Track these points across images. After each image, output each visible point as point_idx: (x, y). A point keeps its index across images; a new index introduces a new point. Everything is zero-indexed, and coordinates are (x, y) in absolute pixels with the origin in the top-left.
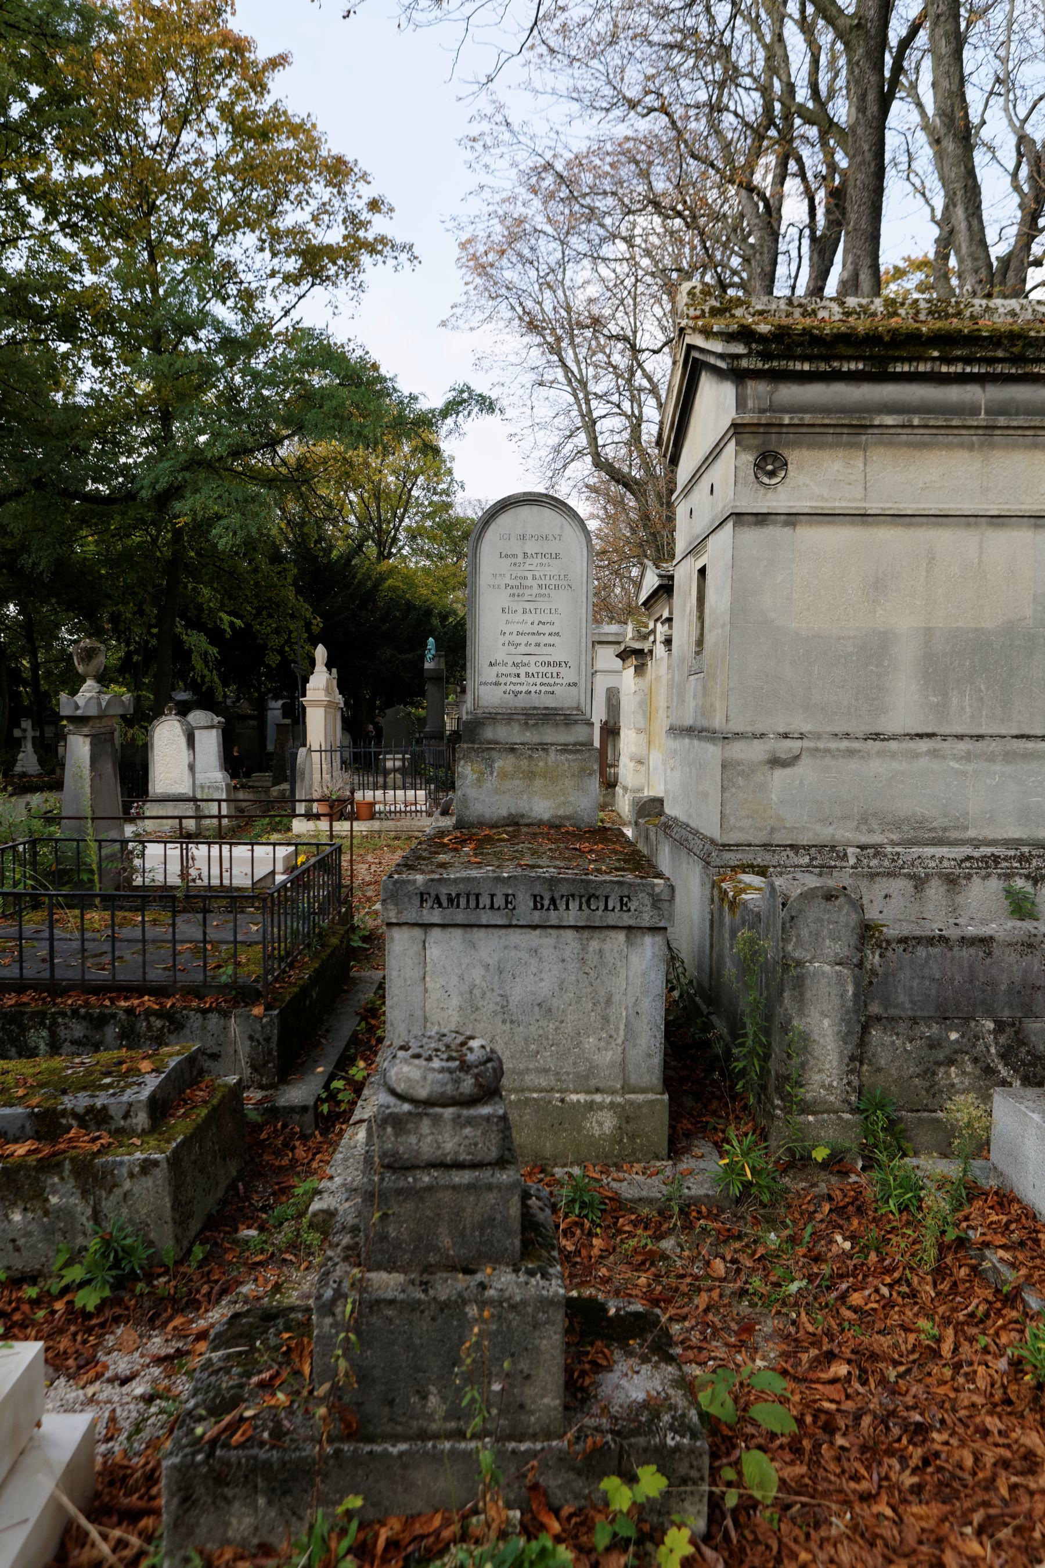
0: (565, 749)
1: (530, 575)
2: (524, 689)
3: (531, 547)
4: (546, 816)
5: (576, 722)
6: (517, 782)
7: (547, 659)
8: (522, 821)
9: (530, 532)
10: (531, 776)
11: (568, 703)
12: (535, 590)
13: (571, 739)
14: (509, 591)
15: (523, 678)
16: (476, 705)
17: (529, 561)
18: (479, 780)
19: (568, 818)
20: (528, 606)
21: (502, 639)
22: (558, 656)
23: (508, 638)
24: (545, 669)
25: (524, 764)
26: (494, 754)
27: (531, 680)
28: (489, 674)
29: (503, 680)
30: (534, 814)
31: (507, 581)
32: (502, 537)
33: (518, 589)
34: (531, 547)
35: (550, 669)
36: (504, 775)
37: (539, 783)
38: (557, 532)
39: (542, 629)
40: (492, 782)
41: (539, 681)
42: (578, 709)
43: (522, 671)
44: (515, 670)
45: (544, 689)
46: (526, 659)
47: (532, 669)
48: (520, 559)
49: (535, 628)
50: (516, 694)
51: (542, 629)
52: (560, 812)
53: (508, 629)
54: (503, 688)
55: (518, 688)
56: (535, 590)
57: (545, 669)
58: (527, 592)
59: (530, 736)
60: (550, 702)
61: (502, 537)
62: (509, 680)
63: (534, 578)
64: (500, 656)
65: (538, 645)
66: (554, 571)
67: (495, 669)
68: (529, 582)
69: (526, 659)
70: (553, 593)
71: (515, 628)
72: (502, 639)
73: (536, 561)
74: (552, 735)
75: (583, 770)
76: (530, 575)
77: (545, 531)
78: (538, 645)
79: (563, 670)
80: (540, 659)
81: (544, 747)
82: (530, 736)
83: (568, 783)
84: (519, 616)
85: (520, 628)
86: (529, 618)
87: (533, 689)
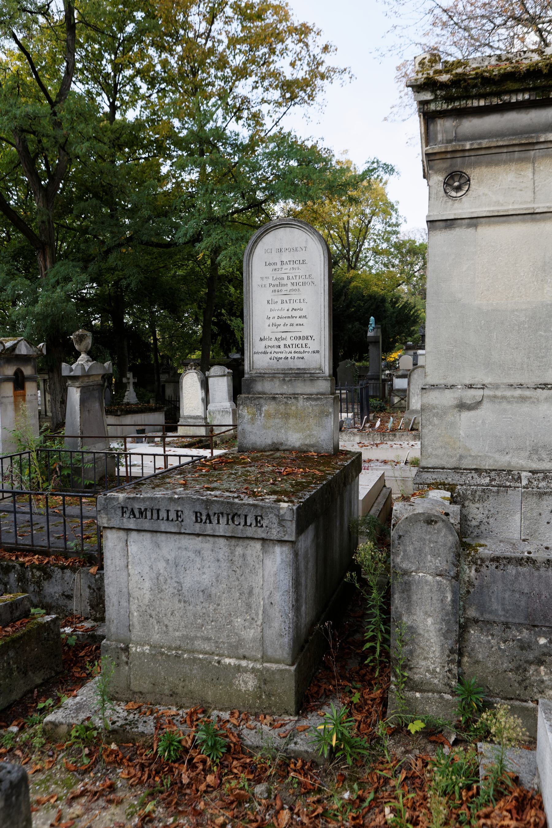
0: (310, 397)
1: (285, 276)
2: (283, 356)
3: (286, 257)
4: (297, 444)
5: (318, 378)
6: (277, 421)
7: (298, 335)
8: (282, 448)
9: (285, 246)
10: (286, 416)
11: (313, 365)
12: (290, 287)
13: (314, 390)
14: (272, 288)
15: (282, 349)
17: (284, 267)
18: (252, 419)
19: (313, 446)
20: (285, 298)
21: (268, 322)
22: (306, 332)
23: (272, 321)
24: (297, 342)
25: (282, 408)
26: (262, 401)
27: (288, 350)
28: (259, 346)
29: (269, 350)
30: (289, 443)
31: (270, 281)
32: (266, 251)
33: (277, 287)
34: (286, 257)
35: (301, 342)
36: (269, 416)
37: (292, 421)
38: (304, 245)
39: (295, 313)
40: (260, 420)
41: (293, 350)
42: (320, 369)
43: (282, 343)
44: (276, 343)
45: (296, 355)
46: (284, 335)
47: (289, 342)
48: (279, 266)
49: (290, 314)
50: (278, 359)
51: (295, 313)
52: (307, 442)
53: (271, 315)
54: (269, 356)
55: (279, 355)
56: (290, 287)
57: (297, 342)
58: (284, 288)
59: (286, 389)
60: (300, 364)
61: (266, 251)
62: (273, 350)
63: (288, 278)
64: (267, 333)
65: (292, 325)
66: (301, 273)
67: (264, 343)
68: (285, 282)
69: (284, 335)
70: (301, 288)
71: (276, 314)
72: (268, 322)
73: (289, 266)
74: (301, 388)
75: (322, 412)
76: (285, 276)
77: (295, 245)
78: (292, 325)
79: (309, 342)
80: (294, 335)
81: (295, 396)
82: (286, 389)
83: (312, 422)
84: (279, 306)
85: (280, 314)
86: (285, 306)
87: (289, 356)
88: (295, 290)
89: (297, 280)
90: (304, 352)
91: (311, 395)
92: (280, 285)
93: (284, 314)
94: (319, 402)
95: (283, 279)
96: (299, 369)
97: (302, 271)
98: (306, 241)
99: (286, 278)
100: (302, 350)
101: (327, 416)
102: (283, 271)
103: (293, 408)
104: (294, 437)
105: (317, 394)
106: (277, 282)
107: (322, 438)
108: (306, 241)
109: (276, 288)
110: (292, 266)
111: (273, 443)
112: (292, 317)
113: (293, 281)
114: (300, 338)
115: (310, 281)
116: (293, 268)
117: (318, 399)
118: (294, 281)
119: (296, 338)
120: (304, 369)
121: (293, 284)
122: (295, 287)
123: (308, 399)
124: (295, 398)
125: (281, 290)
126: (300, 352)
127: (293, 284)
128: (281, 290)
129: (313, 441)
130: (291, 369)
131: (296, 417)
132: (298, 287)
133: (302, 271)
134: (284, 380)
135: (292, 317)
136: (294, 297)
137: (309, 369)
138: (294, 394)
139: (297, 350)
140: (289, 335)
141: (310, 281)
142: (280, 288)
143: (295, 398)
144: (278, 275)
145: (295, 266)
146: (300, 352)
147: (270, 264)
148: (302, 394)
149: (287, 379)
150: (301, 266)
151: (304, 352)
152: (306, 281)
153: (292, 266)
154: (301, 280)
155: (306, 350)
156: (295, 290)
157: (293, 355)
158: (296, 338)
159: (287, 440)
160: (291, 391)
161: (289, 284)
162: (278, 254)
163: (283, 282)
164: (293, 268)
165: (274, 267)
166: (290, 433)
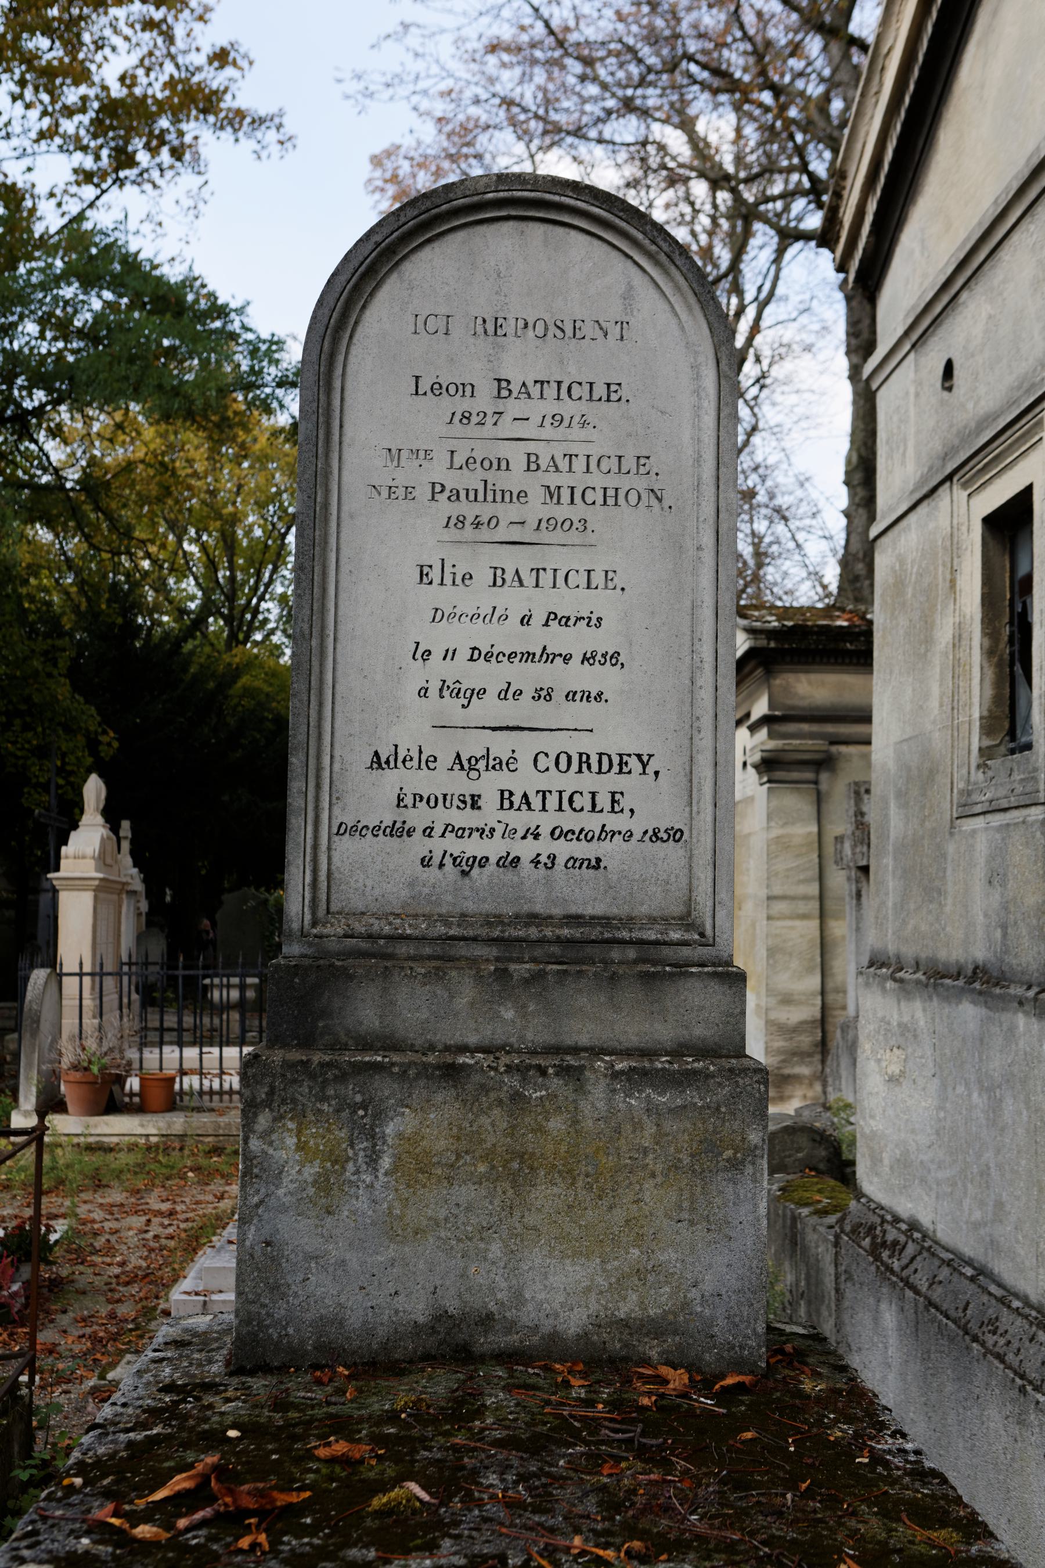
0: (642, 1067)
1: (516, 454)
2: (493, 848)
3: (521, 362)
4: (574, 1322)
5: (681, 969)
6: (465, 1193)
7: (575, 744)
8: (486, 1342)
9: (517, 308)
10: (516, 1169)
11: (652, 901)
12: (537, 508)
13: (663, 1032)
14: (445, 507)
15: (490, 814)
16: (321, 908)
17: (514, 407)
18: (323, 1184)
19: (655, 1328)
20: (511, 560)
21: (417, 674)
22: (614, 732)
23: (437, 669)
24: (569, 782)
25: (493, 1124)
26: (385, 1088)
27: (520, 820)
28: (370, 797)
29: (418, 817)
30: (528, 1315)
31: (438, 471)
32: (421, 324)
33: (475, 503)
34: (521, 362)
35: (588, 781)
36: (417, 1167)
37: (547, 1195)
38: (614, 310)
39: (559, 639)
40: (371, 1193)
41: (546, 822)
42: (687, 920)
43: (489, 785)
44: (460, 784)
45: (564, 849)
46: (501, 745)
47: (524, 780)
48: (484, 401)
49: (535, 638)
50: (467, 866)
51: (559, 639)
52: (628, 1307)
53: (438, 638)
54: (419, 846)
55: (474, 847)
56: (537, 508)
57: (569, 782)
58: (508, 512)
59: (513, 1022)
60: (586, 897)
61: (421, 324)
62: (442, 816)
63: (532, 464)
64: (409, 732)
65: (543, 695)
66: (600, 442)
67: (392, 780)
68: (515, 479)
69: (501, 745)
70: (596, 516)
71: (464, 636)
72: (417, 674)
73: (536, 409)
74: (595, 1018)
75: (709, 1147)
76: (516, 454)
77: (572, 307)
78: (543, 695)
79: (632, 785)
80: (553, 744)
81: (567, 1062)
82: (513, 1022)
83: (655, 1197)
84: (479, 597)
85: (483, 636)
86: (513, 600)
87: (526, 850)
88: (567, 524)
89: (579, 479)
90: (605, 834)
91: (647, 1053)
92: (488, 493)
93: (507, 637)
94: (692, 1096)
95: (502, 464)
96: (574, 920)
97: (602, 434)
98: (628, 296)
99: (518, 463)
100: (593, 823)
101: (735, 1165)
102: (507, 428)
103: (556, 1124)
104: (556, 1280)
105: (678, 1052)
106: (473, 480)
107: (708, 1286)
108: (628, 296)
109: (468, 510)
110: (550, 407)
111: (441, 1317)
112: (547, 656)
113: (553, 480)
114: (584, 760)
115: (641, 484)
116: (558, 420)
117: (690, 1077)
118: (564, 480)
119: (563, 761)
120: (605, 921)
121: (553, 494)
122: (563, 512)
123: (637, 1078)
124: (572, 1074)
125: (493, 521)
126: (584, 836)
127: (553, 494)
128: (493, 521)
129: (659, 1301)
130: (534, 919)
131: (570, 1175)
132: (578, 511)
133: (602, 434)
134: (503, 974)
135: (547, 656)
136: (558, 559)
137: (628, 922)
138: (556, 1050)
139: (569, 821)
140: (526, 745)
141: (641, 484)
142: (485, 511)
143: (564, 1071)
144: (475, 443)
145: (568, 408)
146: (584, 836)
147: (437, 389)
148: (597, 1052)
149: (520, 969)
150: (596, 412)
151: (605, 834)
152: (624, 483)
153: (550, 407)
154: (597, 480)
155: (614, 822)
156: (567, 524)
157: (545, 846)
158: (563, 761)
159: (518, 1297)
160: (537, 1032)
161: (537, 495)
162: (483, 345)
163: (502, 481)
164: (558, 420)
165: (462, 405)
166: (536, 1257)
